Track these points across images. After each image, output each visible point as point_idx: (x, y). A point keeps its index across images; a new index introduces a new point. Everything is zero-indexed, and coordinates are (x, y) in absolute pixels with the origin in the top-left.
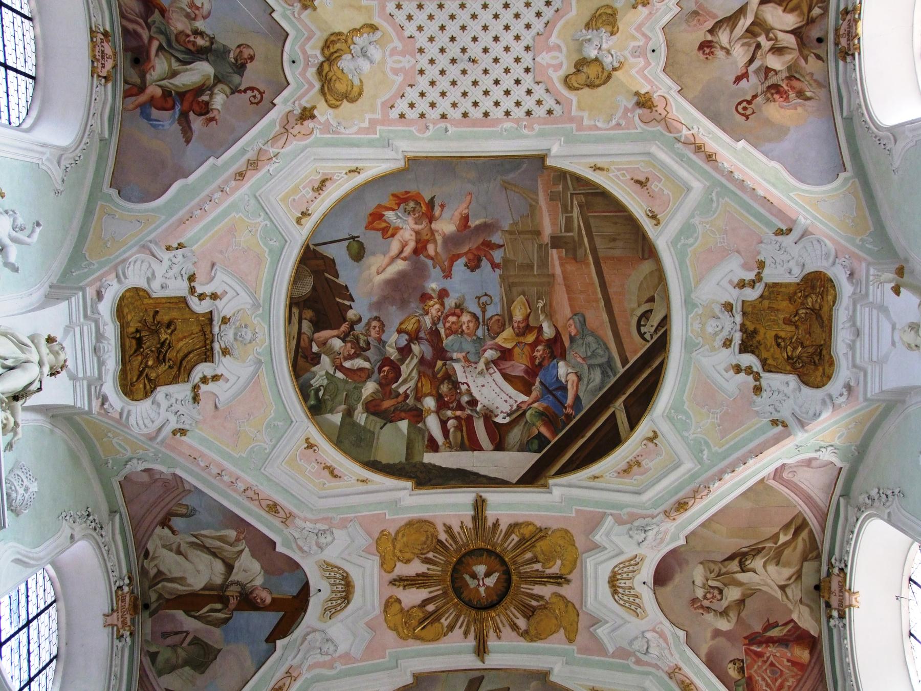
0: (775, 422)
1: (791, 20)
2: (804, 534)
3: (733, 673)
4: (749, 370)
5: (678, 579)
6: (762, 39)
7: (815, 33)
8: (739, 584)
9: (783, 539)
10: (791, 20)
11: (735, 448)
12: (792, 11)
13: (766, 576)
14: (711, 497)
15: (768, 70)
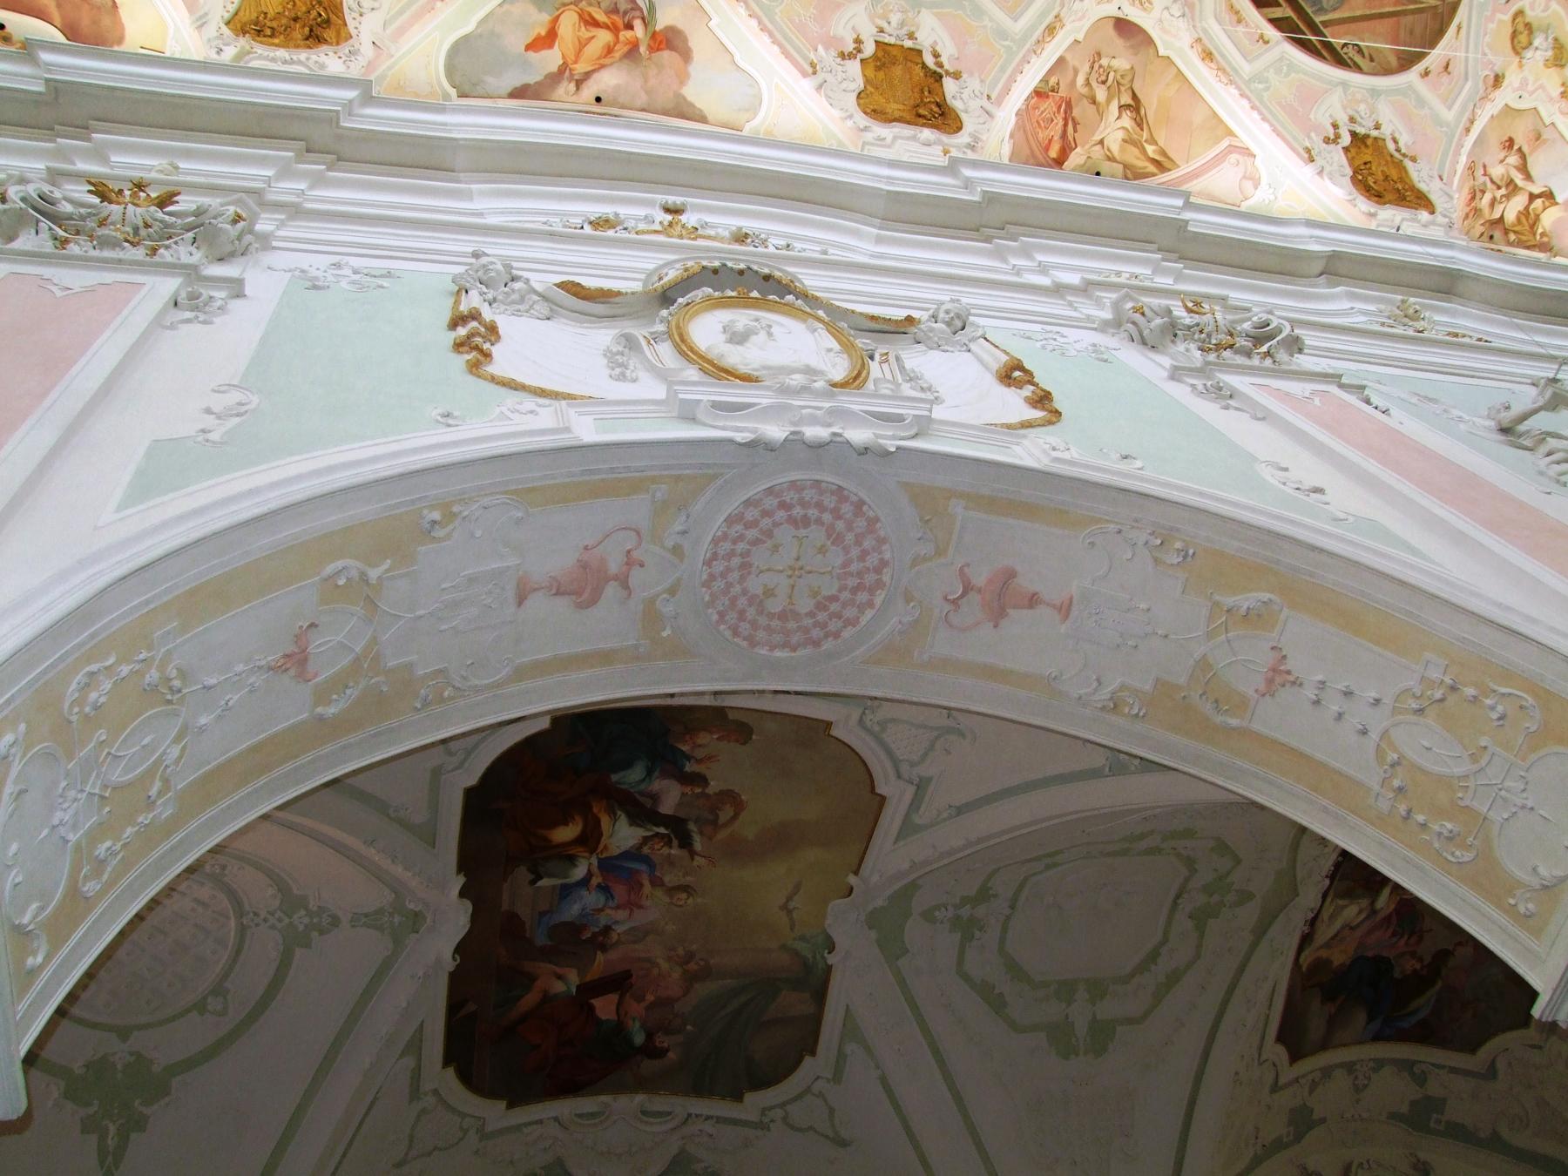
0: (1308, 151)
1: (1510, 217)
2: (1152, 168)
3: (1053, 81)
4: (1337, 136)
5: (1119, 42)
6: (1503, 191)
7: (1497, 234)
8: (1109, 101)
9: (1150, 149)
10: (1510, 217)
11: (1271, 112)
12: (1518, 219)
13: (1114, 129)
14: (1218, 86)
15: (1483, 192)
